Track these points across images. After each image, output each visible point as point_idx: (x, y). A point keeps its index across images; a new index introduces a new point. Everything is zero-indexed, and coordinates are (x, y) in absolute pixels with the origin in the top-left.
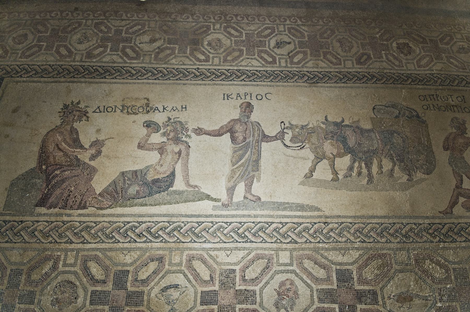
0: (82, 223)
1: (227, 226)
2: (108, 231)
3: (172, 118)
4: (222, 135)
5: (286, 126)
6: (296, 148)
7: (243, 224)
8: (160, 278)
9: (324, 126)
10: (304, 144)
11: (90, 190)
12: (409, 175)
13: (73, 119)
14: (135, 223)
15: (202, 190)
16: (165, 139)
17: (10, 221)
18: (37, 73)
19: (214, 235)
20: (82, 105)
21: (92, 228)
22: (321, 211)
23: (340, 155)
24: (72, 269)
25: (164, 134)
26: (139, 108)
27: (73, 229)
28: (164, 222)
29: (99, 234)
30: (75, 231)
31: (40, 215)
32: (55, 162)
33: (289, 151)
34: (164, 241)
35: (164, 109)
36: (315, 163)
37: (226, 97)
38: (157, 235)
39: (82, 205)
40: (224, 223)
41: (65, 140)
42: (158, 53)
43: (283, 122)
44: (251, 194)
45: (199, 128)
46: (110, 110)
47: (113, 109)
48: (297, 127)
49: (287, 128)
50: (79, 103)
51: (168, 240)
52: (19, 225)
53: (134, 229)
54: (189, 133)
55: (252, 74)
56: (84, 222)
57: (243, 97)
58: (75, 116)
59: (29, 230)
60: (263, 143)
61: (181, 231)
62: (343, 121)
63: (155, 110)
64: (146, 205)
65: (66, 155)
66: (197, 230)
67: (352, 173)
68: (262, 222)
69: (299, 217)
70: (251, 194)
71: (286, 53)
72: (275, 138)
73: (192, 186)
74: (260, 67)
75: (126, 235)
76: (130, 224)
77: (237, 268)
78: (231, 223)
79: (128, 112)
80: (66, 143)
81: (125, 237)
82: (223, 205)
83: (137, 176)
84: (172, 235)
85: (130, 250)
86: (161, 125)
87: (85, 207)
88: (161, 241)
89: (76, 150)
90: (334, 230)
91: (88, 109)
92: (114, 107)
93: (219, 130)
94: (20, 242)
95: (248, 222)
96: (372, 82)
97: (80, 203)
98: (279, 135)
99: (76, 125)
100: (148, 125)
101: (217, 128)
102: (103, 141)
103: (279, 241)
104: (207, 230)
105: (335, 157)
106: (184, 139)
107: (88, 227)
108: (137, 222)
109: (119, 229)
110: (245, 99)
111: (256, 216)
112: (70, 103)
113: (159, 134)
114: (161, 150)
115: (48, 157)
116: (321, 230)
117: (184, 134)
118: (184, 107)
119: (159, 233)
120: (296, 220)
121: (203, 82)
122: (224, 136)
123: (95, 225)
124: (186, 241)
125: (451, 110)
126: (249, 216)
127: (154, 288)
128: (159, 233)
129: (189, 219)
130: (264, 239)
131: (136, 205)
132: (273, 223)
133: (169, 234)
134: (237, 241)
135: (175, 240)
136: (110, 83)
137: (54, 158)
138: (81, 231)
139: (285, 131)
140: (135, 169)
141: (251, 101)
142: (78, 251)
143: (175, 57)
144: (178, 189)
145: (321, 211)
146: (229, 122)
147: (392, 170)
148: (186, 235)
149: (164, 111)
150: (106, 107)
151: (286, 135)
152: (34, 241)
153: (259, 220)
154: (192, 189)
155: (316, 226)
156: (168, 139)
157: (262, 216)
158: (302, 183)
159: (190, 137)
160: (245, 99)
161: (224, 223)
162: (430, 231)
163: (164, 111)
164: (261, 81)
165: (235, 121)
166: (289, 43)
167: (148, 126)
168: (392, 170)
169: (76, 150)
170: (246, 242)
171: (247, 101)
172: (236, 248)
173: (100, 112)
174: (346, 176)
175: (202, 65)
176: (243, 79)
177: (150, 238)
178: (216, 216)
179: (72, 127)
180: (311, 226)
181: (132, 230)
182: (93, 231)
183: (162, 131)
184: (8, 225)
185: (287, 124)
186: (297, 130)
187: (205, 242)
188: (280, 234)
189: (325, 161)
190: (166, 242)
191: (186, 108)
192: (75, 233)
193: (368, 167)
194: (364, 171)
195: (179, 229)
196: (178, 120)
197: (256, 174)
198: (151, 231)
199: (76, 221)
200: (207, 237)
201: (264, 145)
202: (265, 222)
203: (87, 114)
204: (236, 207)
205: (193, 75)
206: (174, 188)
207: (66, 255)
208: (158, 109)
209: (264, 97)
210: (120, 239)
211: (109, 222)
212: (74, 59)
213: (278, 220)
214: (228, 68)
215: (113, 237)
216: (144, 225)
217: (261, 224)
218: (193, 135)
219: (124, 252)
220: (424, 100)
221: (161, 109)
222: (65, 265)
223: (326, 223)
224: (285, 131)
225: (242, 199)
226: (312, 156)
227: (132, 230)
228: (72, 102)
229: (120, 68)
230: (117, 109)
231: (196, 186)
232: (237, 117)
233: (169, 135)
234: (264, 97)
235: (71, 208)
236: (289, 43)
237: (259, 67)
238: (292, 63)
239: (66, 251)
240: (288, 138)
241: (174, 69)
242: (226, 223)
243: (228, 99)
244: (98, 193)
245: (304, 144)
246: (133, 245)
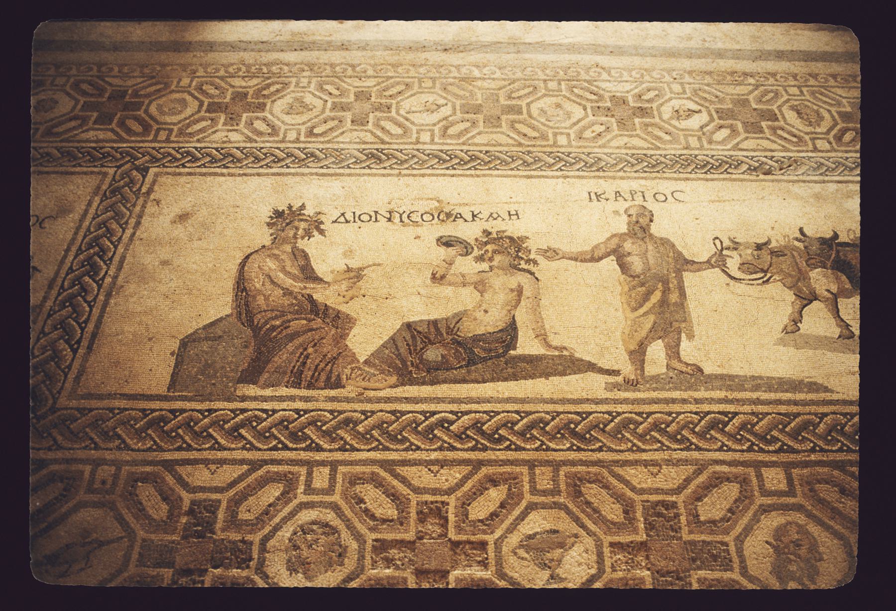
0: (336, 414)
1: (641, 419)
2: (391, 428)
3: (494, 231)
4: (600, 259)
6: (754, 282)
7: (674, 415)
8: (517, 519)
10: (769, 275)
11: (343, 354)
13: (296, 234)
14: (447, 414)
15: (577, 355)
16: (485, 266)
17: (185, 411)
18: (214, 160)
19: (615, 434)
20: (309, 211)
21: (357, 423)
22: (832, 391)
24: (327, 499)
25: (480, 259)
26: (422, 215)
27: (319, 424)
28: (508, 412)
29: (375, 433)
30: (324, 428)
31: (244, 399)
32: (267, 306)
33: (741, 288)
34: (513, 447)
35: (474, 216)
36: (797, 307)
37: (593, 197)
38: (496, 436)
39: (333, 379)
40: (636, 413)
41: (283, 270)
42: (446, 128)
43: (717, 238)
44: (680, 361)
45: (549, 249)
46: (365, 218)
47: (371, 217)
49: (728, 248)
50: (303, 207)
51: (523, 445)
52: (205, 417)
53: (446, 425)
54: (532, 257)
56: (340, 412)
57: (628, 196)
58: (297, 228)
59: (226, 426)
60: (685, 274)
61: (547, 428)
62: (836, 236)
63: (456, 217)
64: (464, 381)
65: (287, 292)
66: (579, 427)
68: (714, 413)
69: (789, 402)
70: (680, 361)
71: (697, 127)
72: (709, 264)
73: (556, 348)
74: (652, 149)
75: (431, 436)
76: (437, 416)
77: (679, 499)
78: (650, 414)
79: (401, 221)
80: (287, 273)
81: (431, 440)
82: (627, 381)
83: (437, 329)
84: (528, 436)
85: (442, 463)
86: (473, 243)
87: (338, 385)
88: (508, 448)
89: (307, 285)
91: (323, 218)
92: (373, 214)
93: (593, 251)
94: (210, 449)
95: (684, 413)
97: (328, 378)
99: (301, 244)
100: (446, 242)
101: (588, 248)
102: (361, 269)
103: (756, 448)
104: (601, 426)
105: (836, 296)
106: (523, 265)
107: (347, 422)
108: (451, 412)
109: (414, 425)
110: (633, 200)
111: (697, 401)
112: (286, 209)
113: (470, 257)
114: (481, 286)
115: (254, 297)
117: (522, 258)
118: (513, 212)
119: (500, 432)
120: (783, 409)
121: (543, 173)
122: (604, 261)
123: (363, 417)
124: (562, 447)
126: (684, 401)
127: (506, 537)
128: (500, 432)
129: (560, 408)
130: (723, 445)
131: (445, 381)
132: (736, 414)
133: (522, 434)
134: (669, 448)
135: (536, 445)
136: (359, 175)
137: (267, 298)
138: (336, 428)
139: (725, 252)
140: (432, 317)
141: (645, 204)
142: (334, 466)
143: (479, 134)
144: (527, 352)
145: (832, 391)
146: (609, 239)
148: (559, 436)
149: (473, 220)
150: (357, 216)
151: (729, 260)
152: (240, 445)
153: (706, 408)
154: (557, 353)
155: (828, 419)
156: (491, 268)
157: (711, 401)
158: (781, 342)
159: (535, 262)
160: (633, 200)
161: (636, 413)
163: (473, 220)
164: (658, 172)
165: (622, 237)
166: (700, 111)
167: (448, 244)
169: (307, 285)
170: (688, 449)
171: (636, 203)
172: (669, 461)
173: (347, 222)
175: (534, 146)
176: (622, 169)
177: (483, 441)
178: (616, 401)
179: (295, 248)
181: (443, 427)
182: (360, 428)
183: (476, 253)
184: (180, 418)
185: (727, 243)
186: (749, 251)
187: (600, 449)
188: (755, 435)
189: (816, 304)
190: (519, 449)
191: (517, 214)
192: (324, 432)
195: (542, 425)
196: (506, 234)
197: (683, 325)
198: (484, 428)
199: (325, 410)
200: (605, 441)
201: (689, 279)
202: (719, 413)
203: (322, 227)
204: (654, 385)
205: (521, 162)
206: (519, 351)
207: (310, 474)
208: (461, 217)
210: (419, 444)
211: (393, 412)
212: (285, 137)
213: (747, 408)
214: (589, 150)
215: (405, 439)
216: (466, 417)
217: (713, 415)
218: (540, 259)
219: (432, 468)
221: (469, 217)
222: (309, 490)
223: (847, 414)
224: (725, 252)
225: (664, 370)
226: (790, 296)
227: (443, 427)
228: (290, 207)
229: (375, 151)
230: (378, 216)
231: (565, 348)
232: (624, 229)
233: (491, 259)
235: (310, 386)
236: (700, 111)
237: (648, 148)
238: (710, 142)
239: (310, 465)
241: (481, 152)
242: (639, 414)
243: (598, 201)
244: (362, 360)
245: (769, 275)
246: (450, 455)
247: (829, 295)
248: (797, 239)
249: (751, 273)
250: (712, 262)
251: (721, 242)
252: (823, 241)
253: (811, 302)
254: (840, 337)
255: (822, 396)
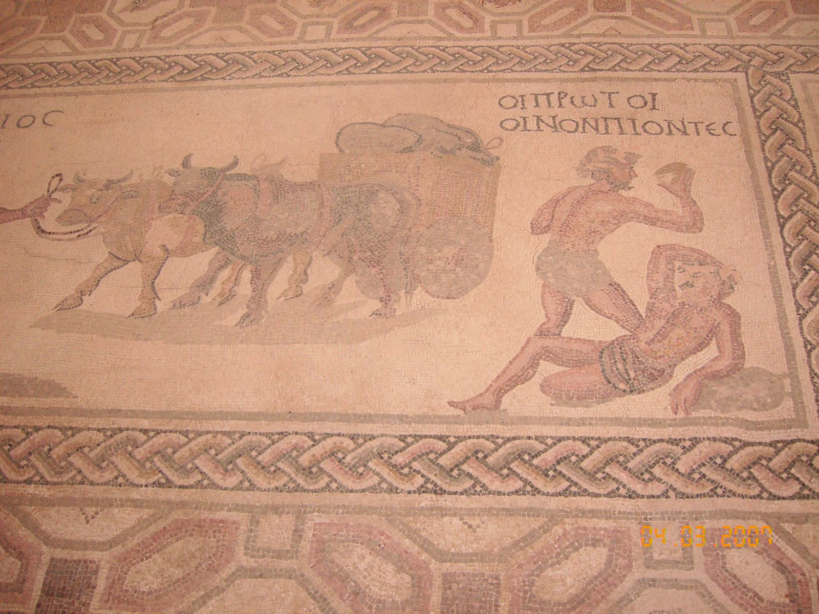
5: (63, 184)
9: (168, 180)
12: (385, 301)
23: (184, 250)
48: (92, 184)
49: (63, 190)
55: (35, 72)
67: (203, 296)
72: (23, 213)
90: (86, 450)
96: (368, 70)
98: (33, 206)
116: (46, 448)
125: (597, 129)
147: (334, 288)
162: (399, 459)
168: (334, 288)
174: (180, 304)
180: (24, 436)
193: (260, 281)
194: (245, 289)
209: (39, 120)
220: (515, 106)
223: (71, 428)
234: (39, 120)
240: (54, 210)
245: (94, 225)
247: (159, 252)
248: (171, 173)
249: (71, 223)
250: (28, 210)
251: (61, 180)
252: (210, 174)
253: (126, 262)
254: (133, 314)
255: (50, 402)
